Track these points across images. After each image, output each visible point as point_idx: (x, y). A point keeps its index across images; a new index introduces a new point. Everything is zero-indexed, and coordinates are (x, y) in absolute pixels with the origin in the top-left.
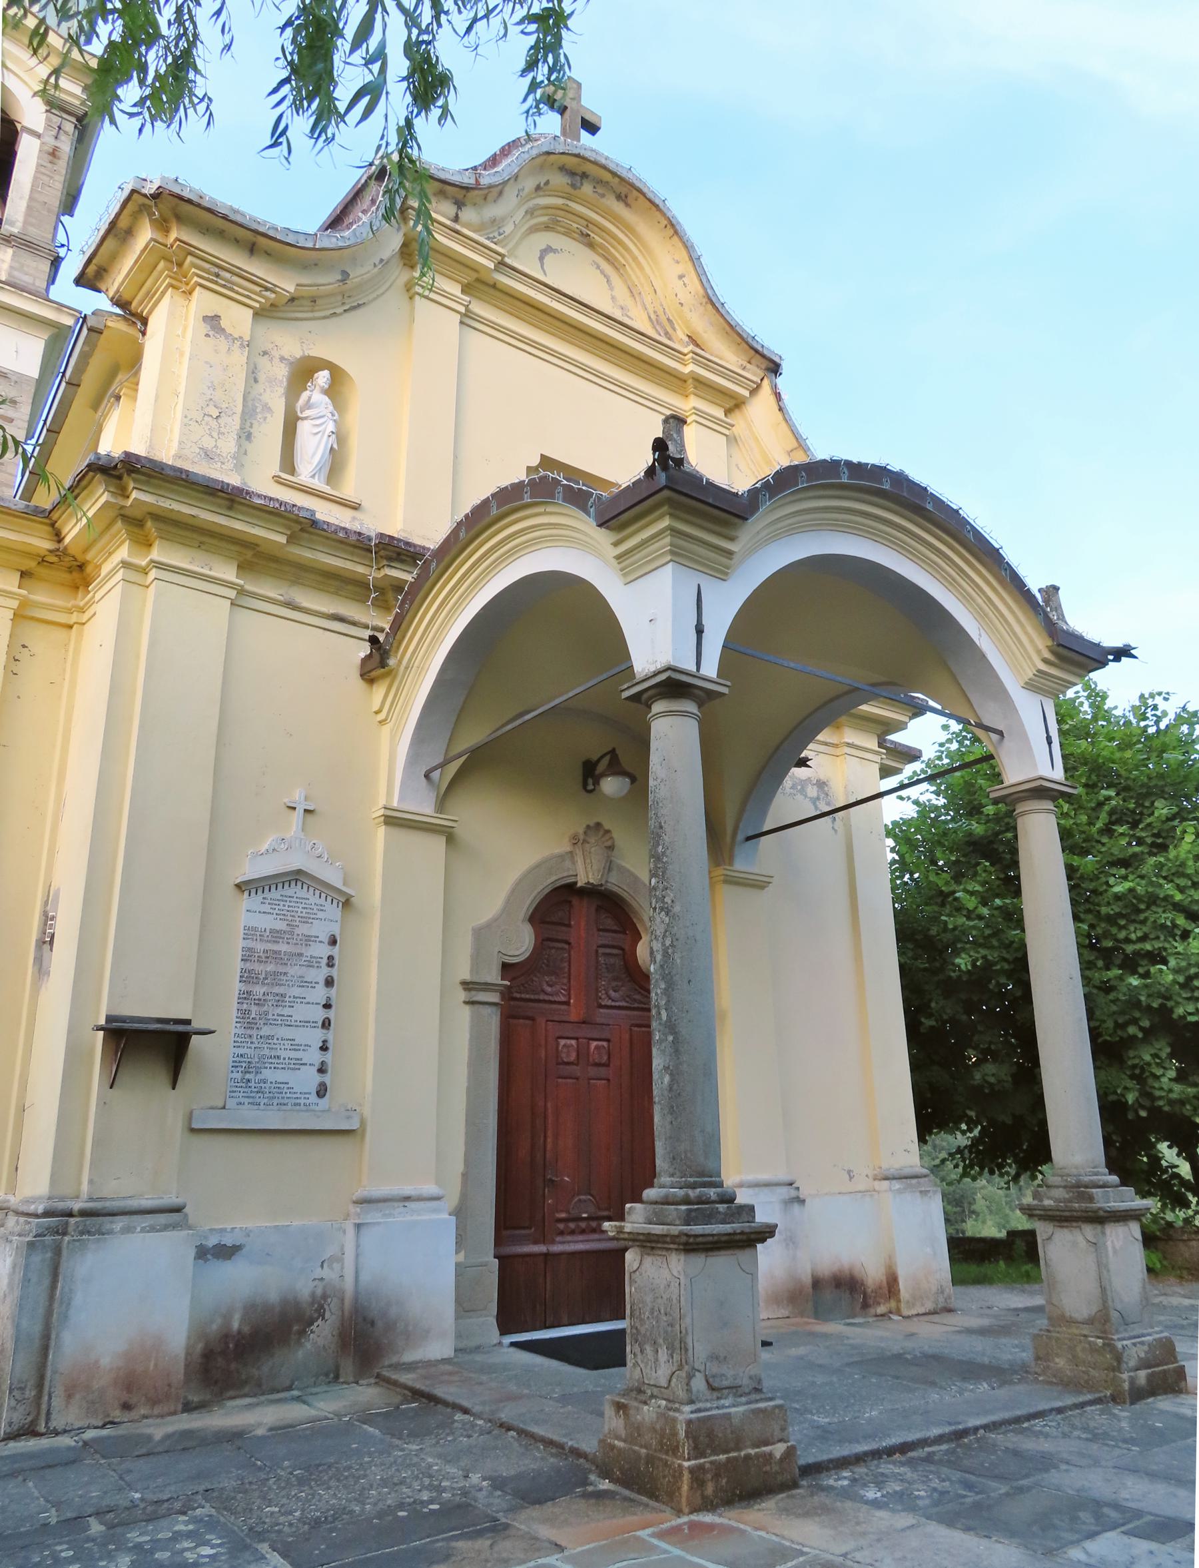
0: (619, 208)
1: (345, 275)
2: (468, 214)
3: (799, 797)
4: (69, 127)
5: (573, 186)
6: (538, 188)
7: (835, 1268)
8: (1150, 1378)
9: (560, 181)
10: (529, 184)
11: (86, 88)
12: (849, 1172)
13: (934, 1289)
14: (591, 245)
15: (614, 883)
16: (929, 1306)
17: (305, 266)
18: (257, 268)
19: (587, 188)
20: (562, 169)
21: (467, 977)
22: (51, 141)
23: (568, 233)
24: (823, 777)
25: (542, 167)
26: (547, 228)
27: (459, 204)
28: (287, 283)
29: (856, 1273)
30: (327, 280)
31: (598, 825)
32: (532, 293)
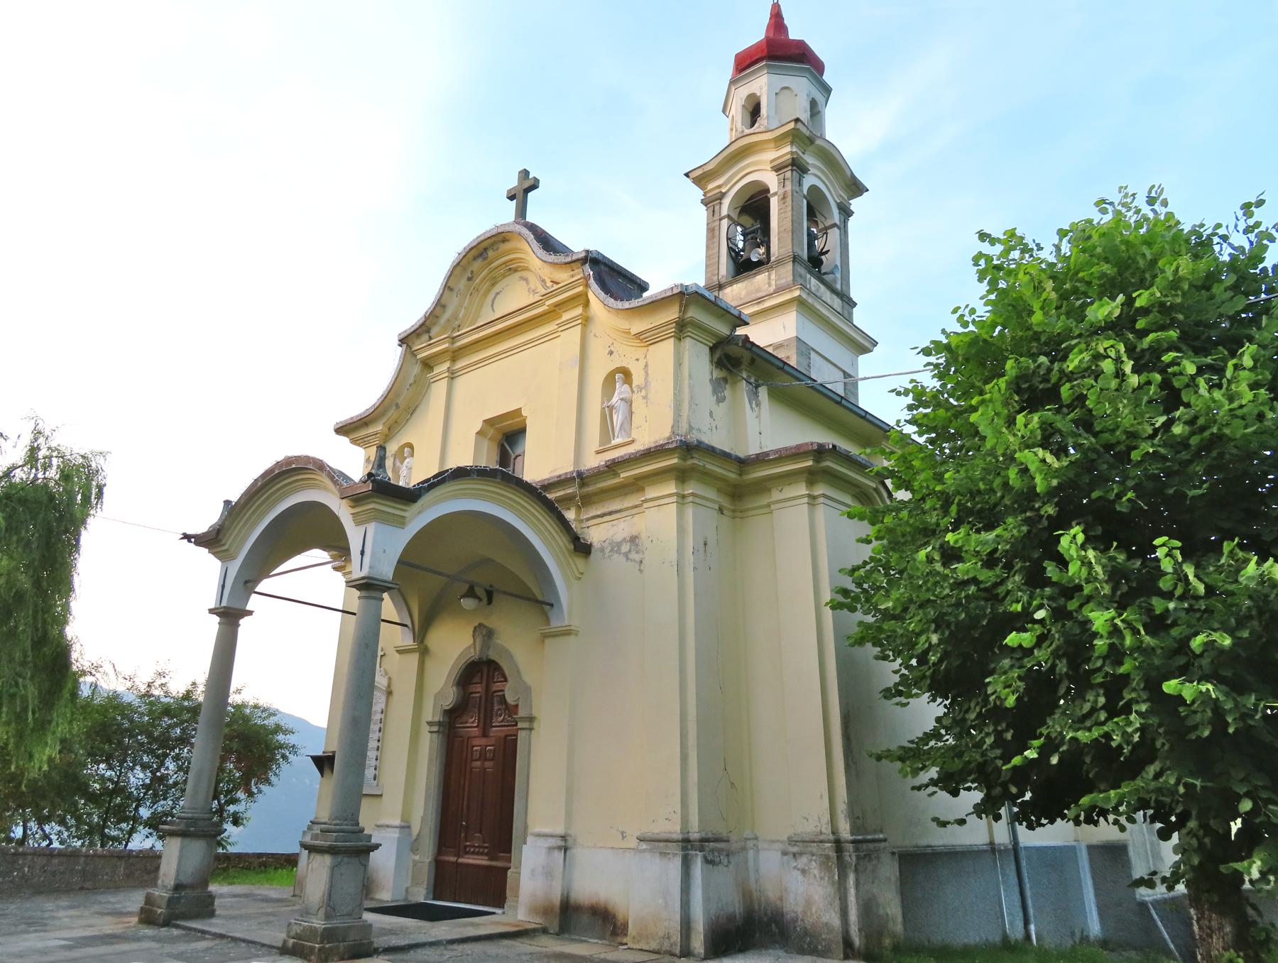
0: (507, 246)
1: (397, 406)
2: (434, 331)
3: (616, 556)
4: (788, 174)
5: (485, 259)
6: (469, 279)
7: (594, 901)
8: (294, 944)
9: (477, 265)
10: (464, 281)
11: (792, 143)
12: (622, 833)
13: (661, 934)
14: (516, 270)
15: (493, 655)
16: (653, 945)
17: (383, 414)
18: (371, 430)
19: (490, 253)
20: (475, 259)
21: (430, 719)
22: (782, 191)
23: (504, 276)
24: (635, 533)
25: (464, 269)
26: (493, 285)
27: (428, 331)
28: (379, 427)
29: (610, 908)
30: (392, 414)
31: (480, 625)
32: (470, 339)
